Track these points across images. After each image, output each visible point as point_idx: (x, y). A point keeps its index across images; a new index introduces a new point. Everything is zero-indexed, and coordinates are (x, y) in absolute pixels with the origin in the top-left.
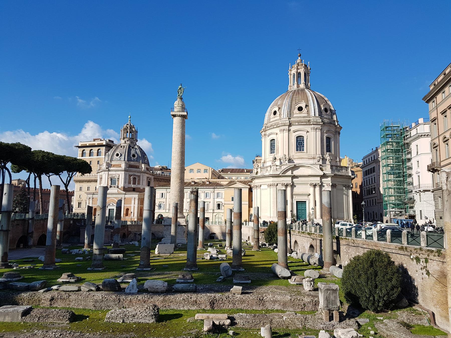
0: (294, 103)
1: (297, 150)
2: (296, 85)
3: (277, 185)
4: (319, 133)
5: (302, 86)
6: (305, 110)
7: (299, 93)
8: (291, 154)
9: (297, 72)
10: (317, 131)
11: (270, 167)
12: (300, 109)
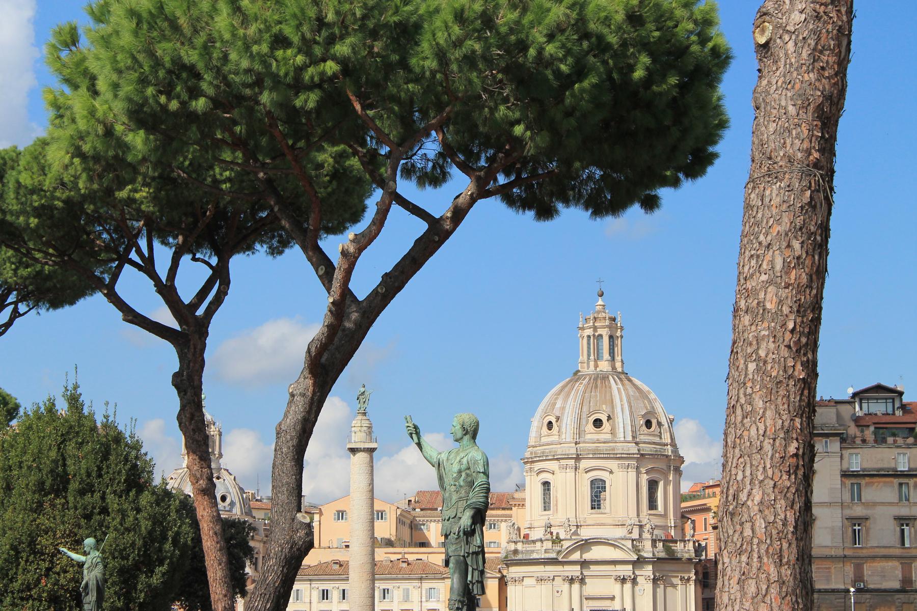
0: (585, 409)
1: (592, 508)
2: (592, 363)
3: (553, 580)
4: (632, 474)
5: (604, 366)
6: (606, 426)
7: (596, 387)
8: (580, 515)
9: (594, 335)
10: (630, 470)
11: (541, 540)
12: (598, 423)
